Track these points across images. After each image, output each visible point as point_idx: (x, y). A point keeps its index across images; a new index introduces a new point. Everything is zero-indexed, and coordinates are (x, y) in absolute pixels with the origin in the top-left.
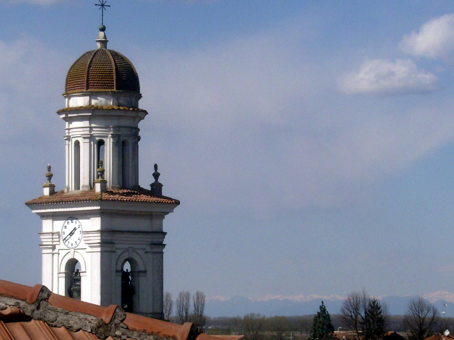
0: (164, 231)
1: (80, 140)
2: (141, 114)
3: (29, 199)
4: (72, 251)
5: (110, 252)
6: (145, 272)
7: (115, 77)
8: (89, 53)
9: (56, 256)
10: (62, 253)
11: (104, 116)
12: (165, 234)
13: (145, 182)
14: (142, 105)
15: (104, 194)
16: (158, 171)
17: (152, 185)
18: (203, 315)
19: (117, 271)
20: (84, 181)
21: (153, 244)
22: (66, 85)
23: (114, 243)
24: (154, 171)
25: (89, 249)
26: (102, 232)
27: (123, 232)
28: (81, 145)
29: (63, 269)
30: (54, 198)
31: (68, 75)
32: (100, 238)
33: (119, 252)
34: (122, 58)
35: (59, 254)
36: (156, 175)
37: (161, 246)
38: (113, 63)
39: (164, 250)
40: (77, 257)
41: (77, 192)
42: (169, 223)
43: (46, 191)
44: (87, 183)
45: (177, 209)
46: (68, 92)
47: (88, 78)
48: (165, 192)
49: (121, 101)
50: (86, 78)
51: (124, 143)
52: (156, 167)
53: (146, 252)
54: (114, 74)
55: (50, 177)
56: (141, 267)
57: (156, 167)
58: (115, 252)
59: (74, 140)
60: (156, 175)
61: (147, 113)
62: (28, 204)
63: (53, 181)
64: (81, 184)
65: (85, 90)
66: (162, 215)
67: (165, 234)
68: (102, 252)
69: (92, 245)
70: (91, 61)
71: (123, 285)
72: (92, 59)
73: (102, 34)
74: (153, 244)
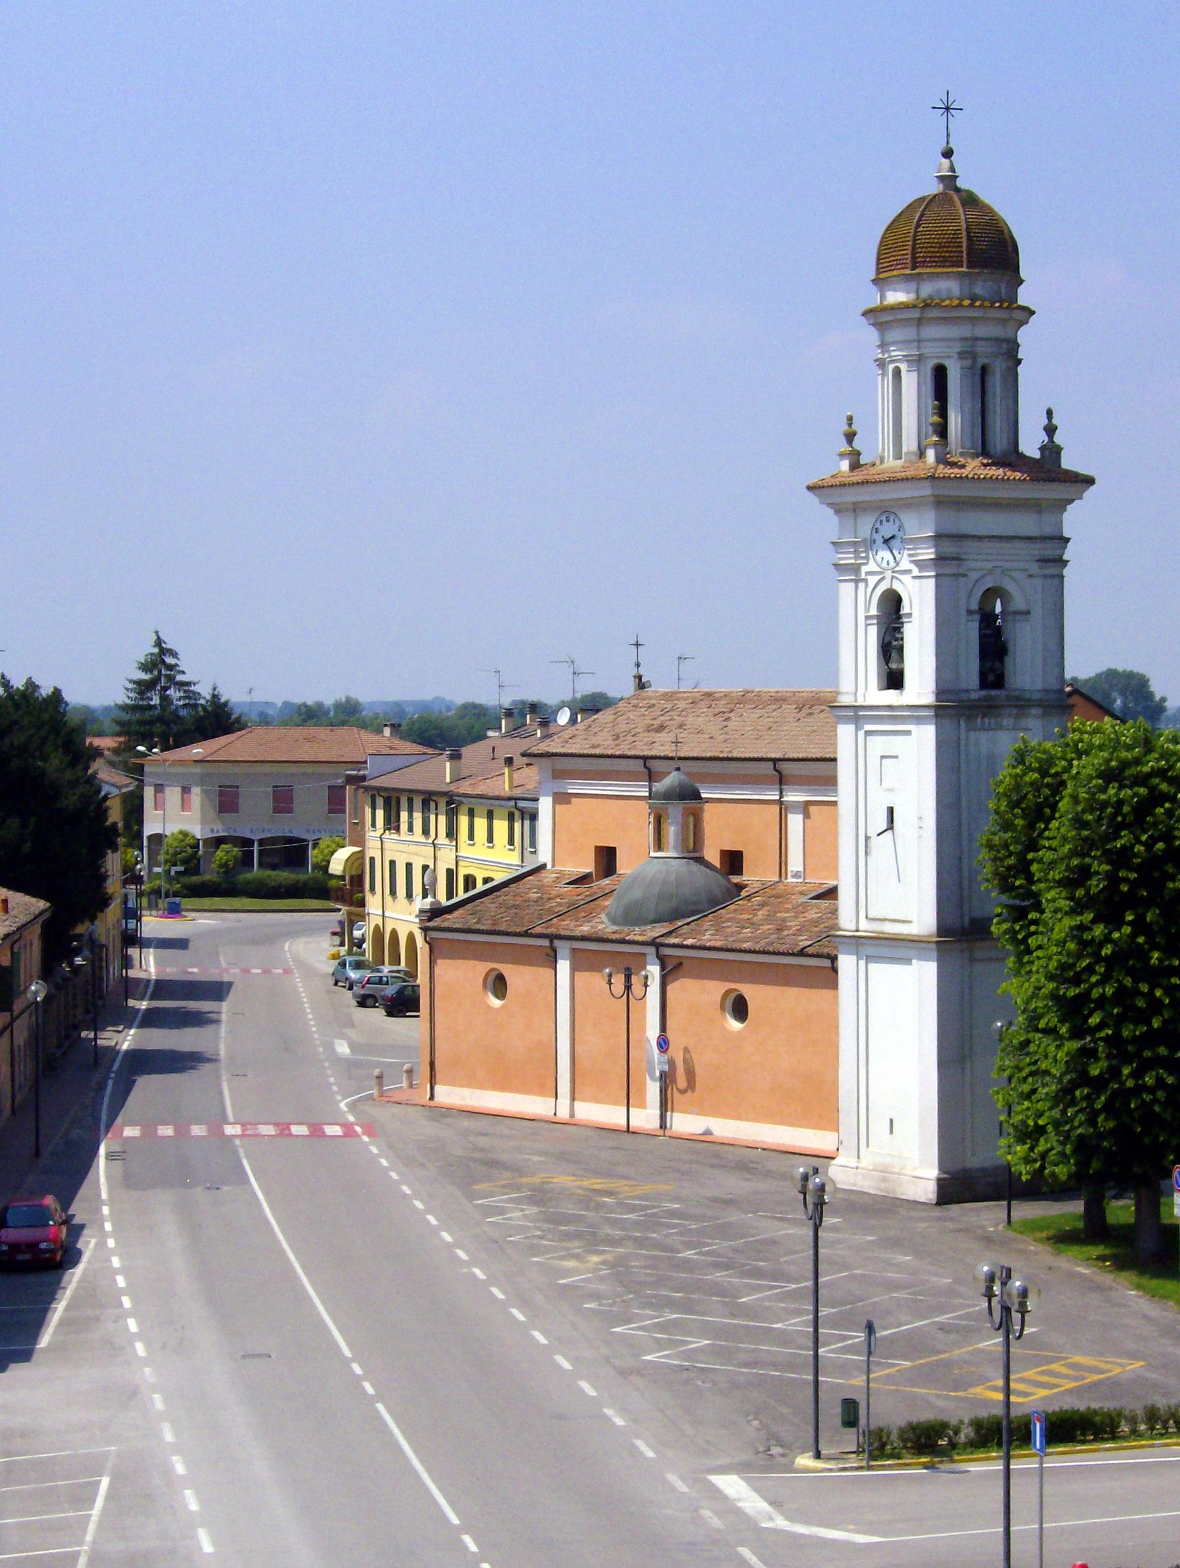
0: (1066, 534)
1: (903, 367)
2: (1017, 315)
3: (812, 481)
4: (888, 574)
5: (954, 575)
6: (1028, 613)
7: (964, 245)
8: (922, 199)
9: (862, 585)
10: (873, 580)
11: (944, 319)
12: (1068, 540)
13: (1030, 444)
14: (1024, 297)
15: (941, 466)
16: (1054, 421)
17: (1042, 449)
18: (1068, 675)
19: (969, 612)
20: (910, 443)
21: (1044, 561)
22: (878, 263)
23: (962, 560)
24: (1046, 422)
25: (916, 572)
26: (939, 538)
27: (980, 538)
28: (903, 374)
29: (874, 611)
30: (858, 476)
31: (881, 242)
32: (933, 550)
33: (974, 576)
34: (987, 210)
35: (866, 581)
36: (1050, 430)
37: (1059, 564)
38: (963, 217)
39: (1066, 572)
40: (897, 587)
41: (900, 463)
42: (1076, 520)
43: (845, 465)
44: (914, 447)
45: (1090, 493)
46: (882, 276)
47: (914, 248)
48: (1067, 463)
49: (978, 290)
50: (910, 248)
51: (984, 370)
52: (1049, 413)
53: (1030, 576)
54: (964, 240)
55: (850, 437)
56: (1018, 603)
57: (1049, 413)
58: (964, 575)
59: (891, 367)
60: (1050, 430)
61: (1033, 313)
62: (809, 488)
63: (857, 444)
64: (904, 450)
65: (908, 272)
66: (1062, 505)
67: (1068, 540)
68: (937, 576)
69: (920, 564)
70: (922, 215)
71: (982, 637)
72: (924, 210)
73: (945, 162)
74: (1044, 561)
